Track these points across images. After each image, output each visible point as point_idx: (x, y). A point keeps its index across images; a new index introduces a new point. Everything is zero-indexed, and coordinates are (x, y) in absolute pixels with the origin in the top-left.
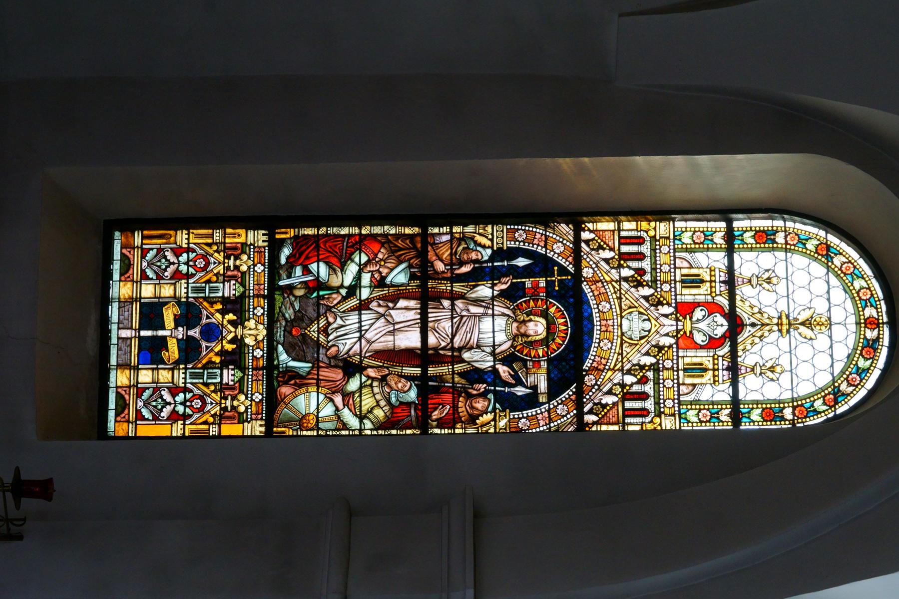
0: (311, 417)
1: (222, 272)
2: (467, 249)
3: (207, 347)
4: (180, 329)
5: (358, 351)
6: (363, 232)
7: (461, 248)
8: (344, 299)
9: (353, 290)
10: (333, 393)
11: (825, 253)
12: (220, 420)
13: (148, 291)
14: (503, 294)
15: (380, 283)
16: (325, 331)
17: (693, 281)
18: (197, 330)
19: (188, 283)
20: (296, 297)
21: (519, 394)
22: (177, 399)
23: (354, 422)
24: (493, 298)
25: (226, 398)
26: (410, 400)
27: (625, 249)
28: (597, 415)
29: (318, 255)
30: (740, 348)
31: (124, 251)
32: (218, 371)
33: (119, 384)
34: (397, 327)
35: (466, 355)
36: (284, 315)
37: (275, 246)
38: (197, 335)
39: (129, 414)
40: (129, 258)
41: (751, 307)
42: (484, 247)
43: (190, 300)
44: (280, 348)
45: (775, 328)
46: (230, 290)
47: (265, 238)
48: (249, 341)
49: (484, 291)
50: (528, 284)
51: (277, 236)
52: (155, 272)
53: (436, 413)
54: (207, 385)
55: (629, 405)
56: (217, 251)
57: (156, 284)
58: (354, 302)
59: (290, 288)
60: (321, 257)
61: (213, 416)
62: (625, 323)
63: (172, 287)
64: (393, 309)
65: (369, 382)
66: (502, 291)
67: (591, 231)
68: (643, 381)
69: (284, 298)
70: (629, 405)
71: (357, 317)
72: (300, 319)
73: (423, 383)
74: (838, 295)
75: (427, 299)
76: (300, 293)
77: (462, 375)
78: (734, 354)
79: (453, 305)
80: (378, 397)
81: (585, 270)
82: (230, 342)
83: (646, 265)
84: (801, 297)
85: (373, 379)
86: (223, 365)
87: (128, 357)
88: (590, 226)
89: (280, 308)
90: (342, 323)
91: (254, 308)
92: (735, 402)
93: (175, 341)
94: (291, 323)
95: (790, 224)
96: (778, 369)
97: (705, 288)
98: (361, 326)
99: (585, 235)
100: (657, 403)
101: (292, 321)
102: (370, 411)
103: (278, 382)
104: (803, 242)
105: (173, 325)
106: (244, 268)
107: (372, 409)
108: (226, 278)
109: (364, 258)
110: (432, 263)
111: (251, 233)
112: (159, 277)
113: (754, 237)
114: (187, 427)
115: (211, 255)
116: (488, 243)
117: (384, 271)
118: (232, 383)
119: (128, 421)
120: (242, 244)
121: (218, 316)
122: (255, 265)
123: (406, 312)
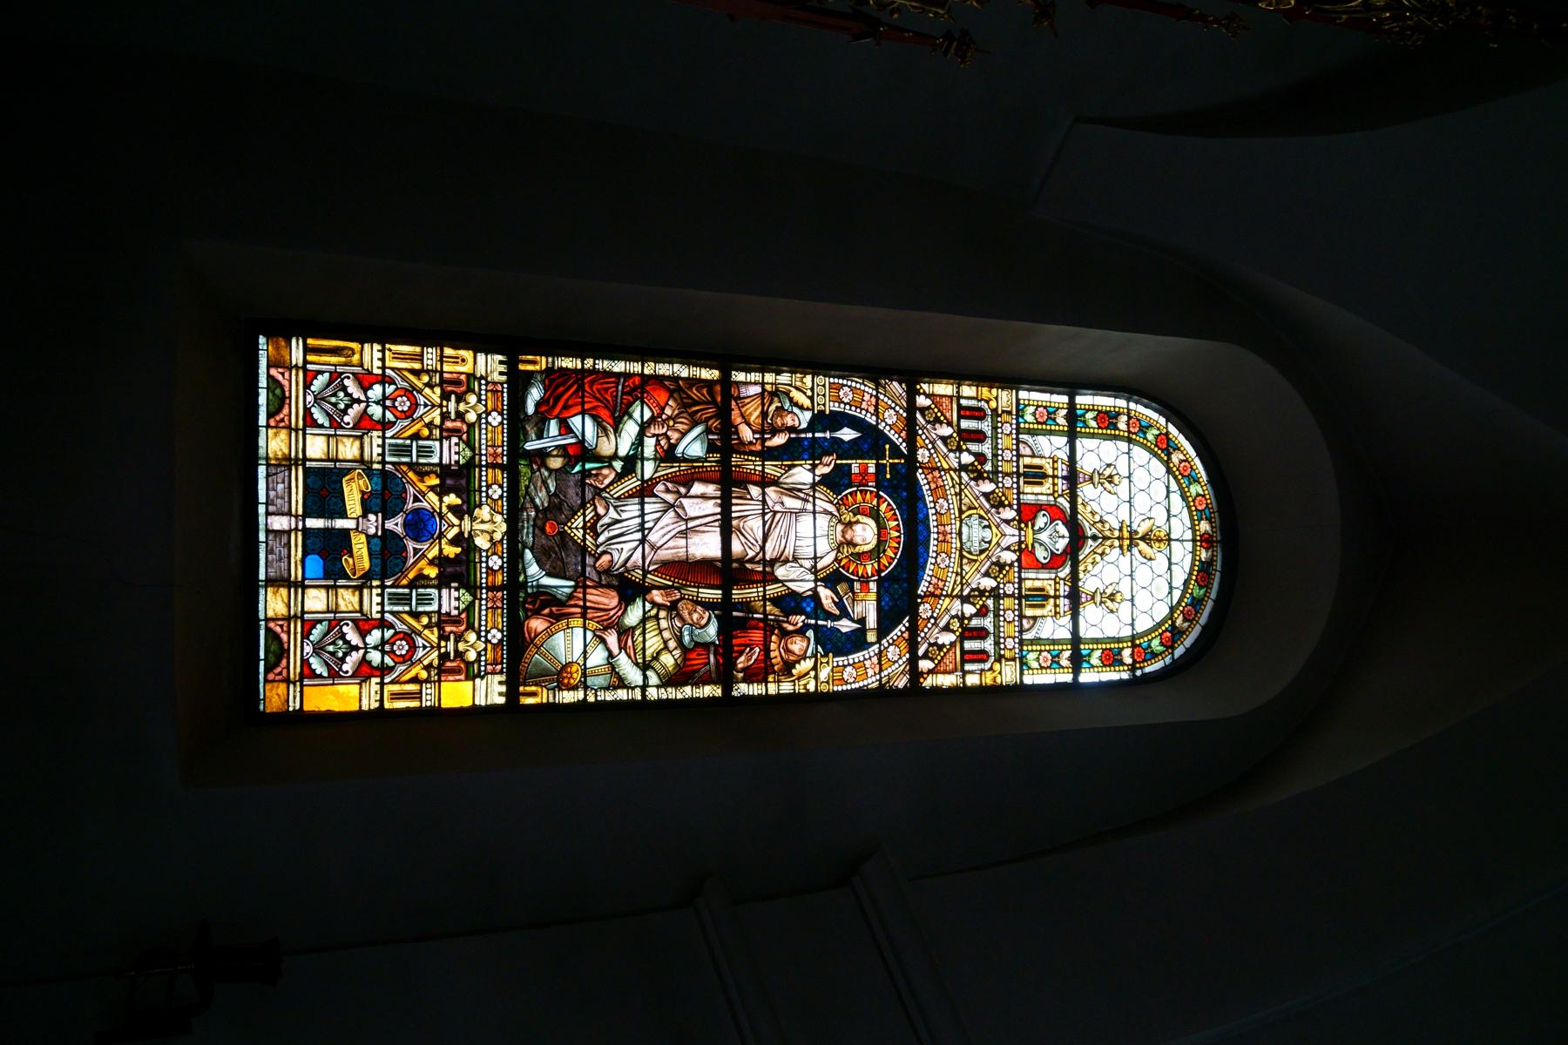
0: (574, 669)
1: (437, 421)
2: (780, 409)
3: (416, 551)
4: (372, 517)
5: (640, 562)
6: (646, 372)
7: (773, 408)
8: (620, 477)
9: (631, 463)
10: (605, 629)
11: (1164, 448)
12: (439, 674)
13: (316, 447)
14: (826, 481)
15: (668, 455)
16: (592, 528)
17: (1036, 476)
18: (400, 519)
19: (384, 438)
20: (550, 471)
21: (844, 630)
22: (369, 639)
23: (634, 675)
24: (814, 486)
25: (447, 639)
26: (708, 640)
27: (965, 424)
28: (932, 660)
29: (583, 403)
30: (1081, 568)
31: (273, 372)
32: (434, 592)
33: (270, 614)
34: (691, 524)
35: (780, 572)
36: (532, 501)
37: (518, 382)
38: (399, 530)
39: (288, 667)
40: (282, 387)
41: (1093, 513)
42: (801, 408)
43: (388, 467)
44: (528, 555)
45: (1116, 543)
46: (450, 452)
47: (503, 368)
48: (482, 542)
49: (801, 475)
50: (855, 470)
51: (522, 367)
52: (328, 414)
53: (742, 659)
54: (416, 615)
55: (968, 645)
56: (430, 385)
57: (329, 436)
58: (631, 483)
59: (542, 455)
60: (587, 406)
61: (428, 668)
62: (965, 530)
63: (357, 443)
64: (685, 496)
65: (653, 612)
66: (824, 476)
67: (928, 396)
68: (983, 612)
69: (533, 472)
70: (968, 645)
71: (638, 507)
72: (557, 509)
73: (723, 610)
74: (1176, 499)
75: (730, 483)
76: (556, 463)
77: (776, 601)
78: (1074, 577)
79: (764, 494)
80: (666, 635)
81: (920, 451)
82: (453, 542)
83: (986, 448)
84: (1141, 503)
85: (659, 606)
86: (443, 582)
87: (284, 565)
88: (925, 387)
89: (527, 487)
90: (616, 516)
91: (489, 487)
92: (1076, 640)
93: (363, 538)
94: (545, 514)
95: (1132, 405)
96: (1118, 597)
97: (1047, 486)
98: (643, 522)
99: (922, 401)
100: (997, 643)
101: (545, 509)
102: (656, 658)
103: (526, 610)
104: (1144, 430)
105: (359, 512)
106: (471, 417)
107: (658, 653)
108: (446, 434)
109: (647, 414)
110: (736, 427)
111: (481, 357)
112: (336, 425)
113: (1095, 419)
114: (387, 688)
115: (420, 392)
116: (807, 403)
117: (674, 436)
118: (455, 612)
119: (287, 681)
120: (468, 375)
121: (432, 497)
122: (488, 414)
123: (702, 502)
